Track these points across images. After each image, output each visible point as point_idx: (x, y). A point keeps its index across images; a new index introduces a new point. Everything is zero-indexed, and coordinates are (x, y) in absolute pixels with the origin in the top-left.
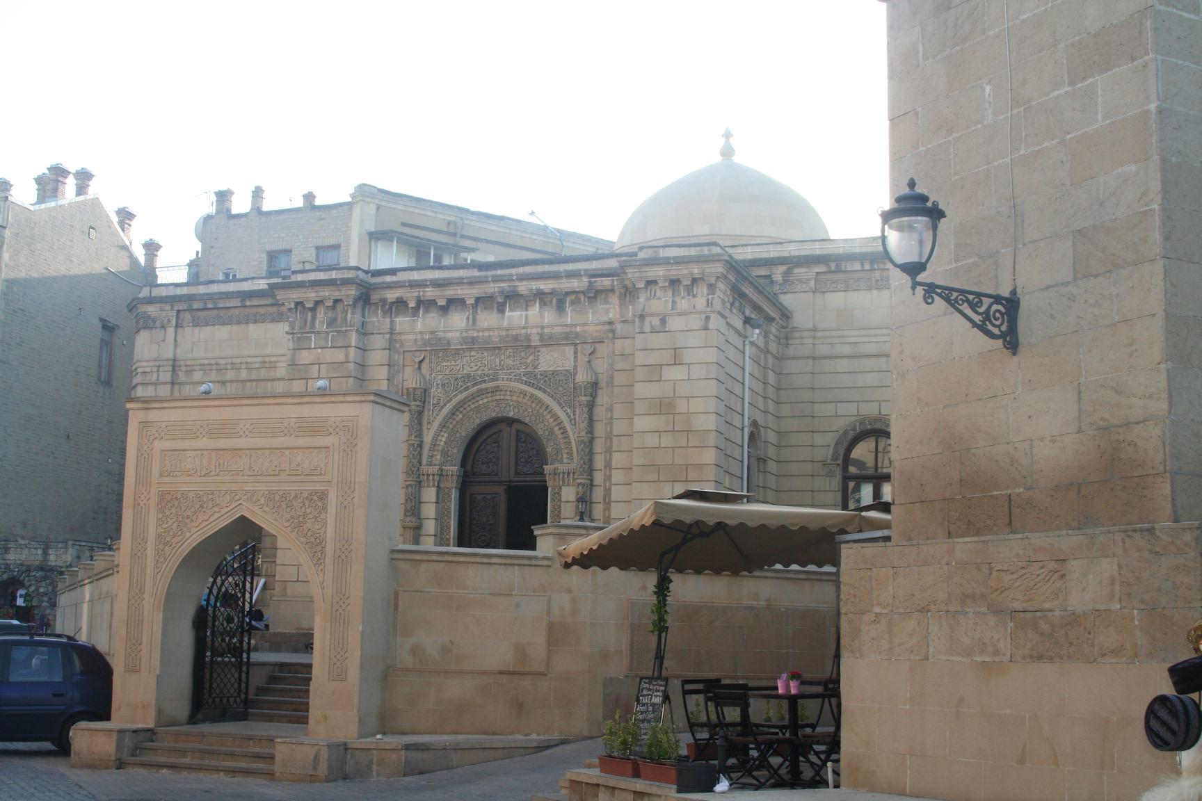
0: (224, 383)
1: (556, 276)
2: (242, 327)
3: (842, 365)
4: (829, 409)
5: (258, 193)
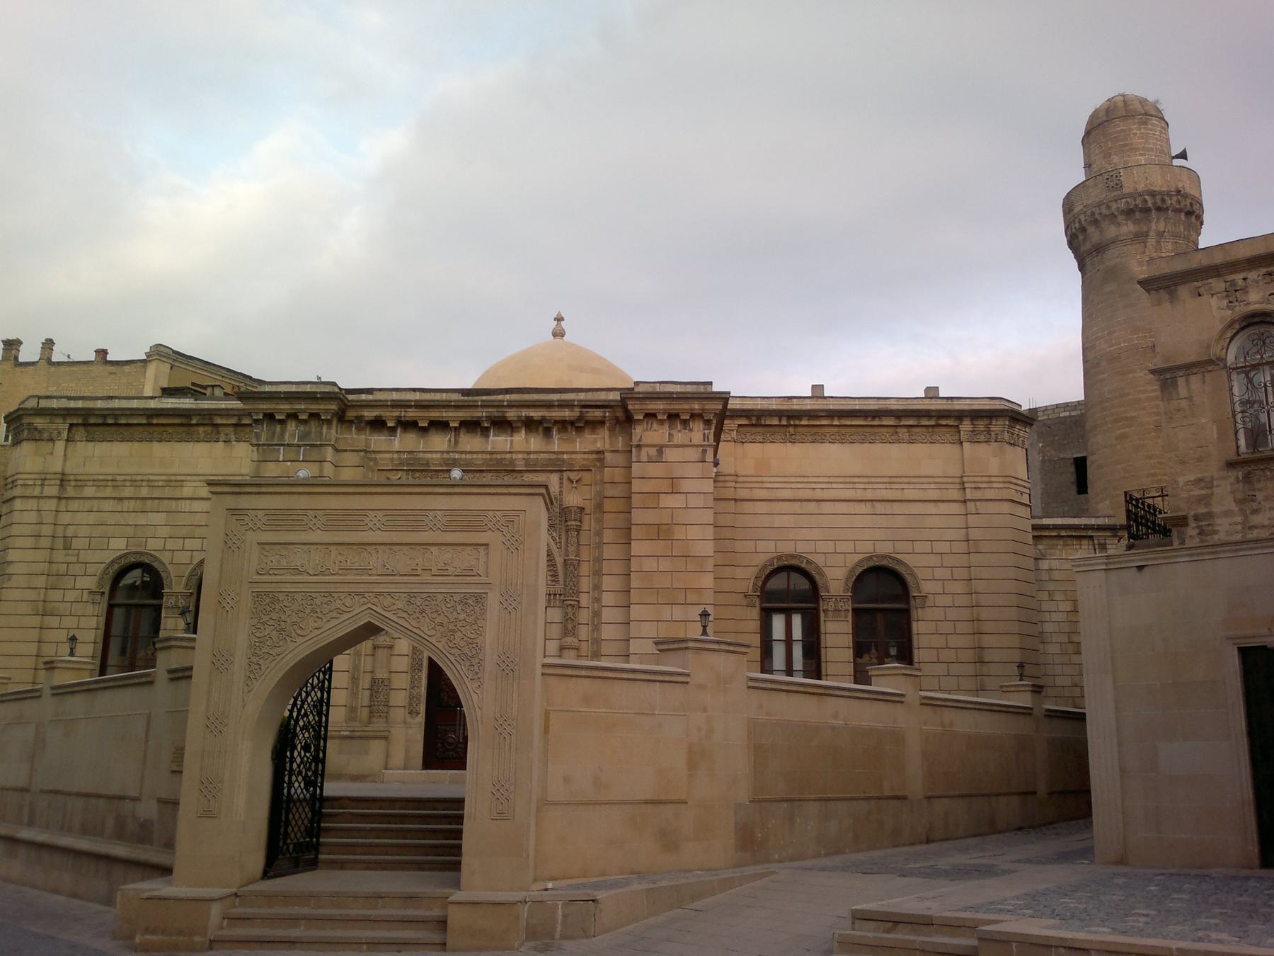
0: (121, 499)
1: (549, 405)
2: (145, 445)
3: (761, 508)
4: (750, 546)
5: (49, 344)
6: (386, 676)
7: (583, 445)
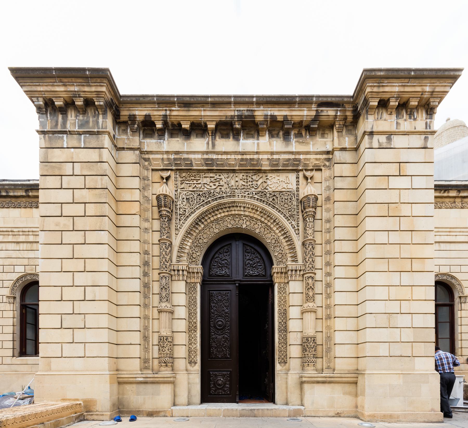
6: (169, 334)
7: (319, 144)
